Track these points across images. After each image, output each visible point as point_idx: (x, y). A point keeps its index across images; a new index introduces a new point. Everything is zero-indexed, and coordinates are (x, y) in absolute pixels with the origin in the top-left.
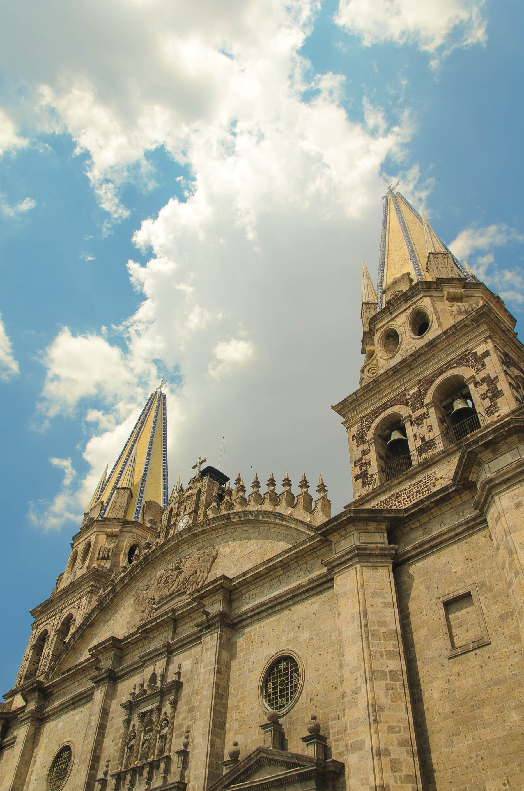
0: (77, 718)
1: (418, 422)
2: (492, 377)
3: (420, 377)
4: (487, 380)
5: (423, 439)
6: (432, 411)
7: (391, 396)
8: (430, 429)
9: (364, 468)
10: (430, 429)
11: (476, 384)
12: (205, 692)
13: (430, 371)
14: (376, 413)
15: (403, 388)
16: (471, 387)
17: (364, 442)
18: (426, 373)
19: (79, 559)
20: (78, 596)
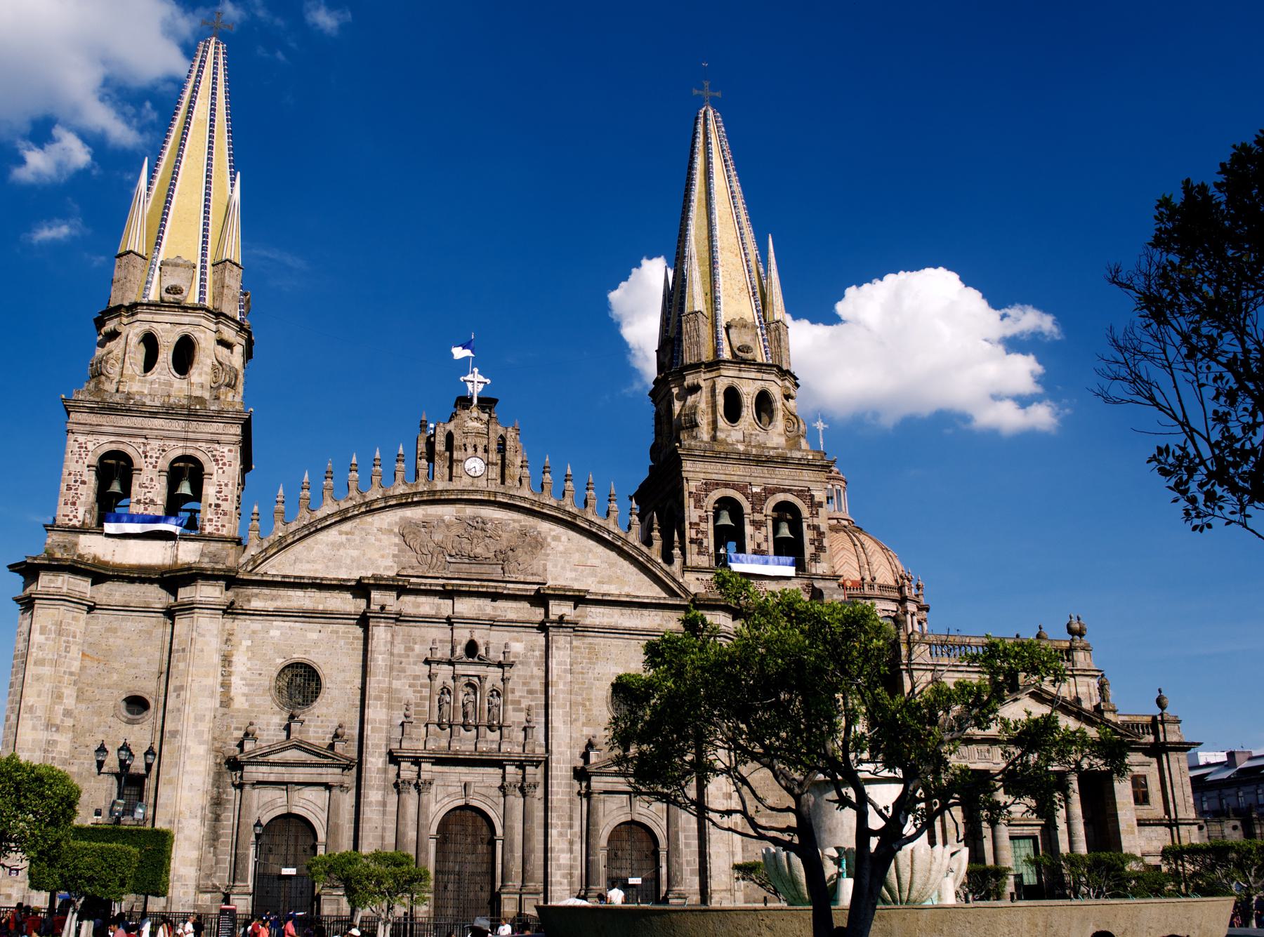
0: (315, 636)
1: (757, 525)
2: (822, 530)
3: (764, 480)
4: (816, 528)
5: (759, 545)
6: (770, 523)
7: (735, 478)
8: (766, 540)
9: (700, 536)
10: (766, 540)
11: (809, 526)
12: (561, 687)
13: (775, 481)
14: (718, 485)
15: (748, 479)
16: (805, 525)
17: (701, 507)
18: (770, 481)
19: (165, 356)
20: (209, 437)
